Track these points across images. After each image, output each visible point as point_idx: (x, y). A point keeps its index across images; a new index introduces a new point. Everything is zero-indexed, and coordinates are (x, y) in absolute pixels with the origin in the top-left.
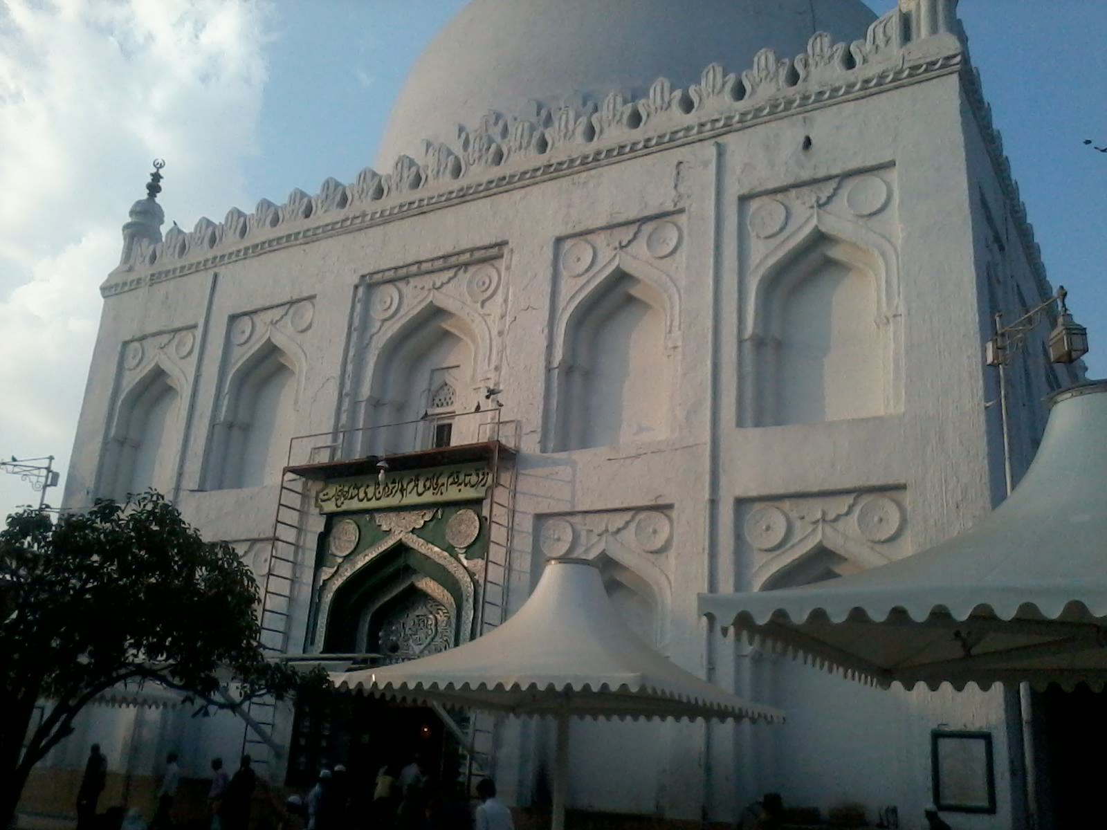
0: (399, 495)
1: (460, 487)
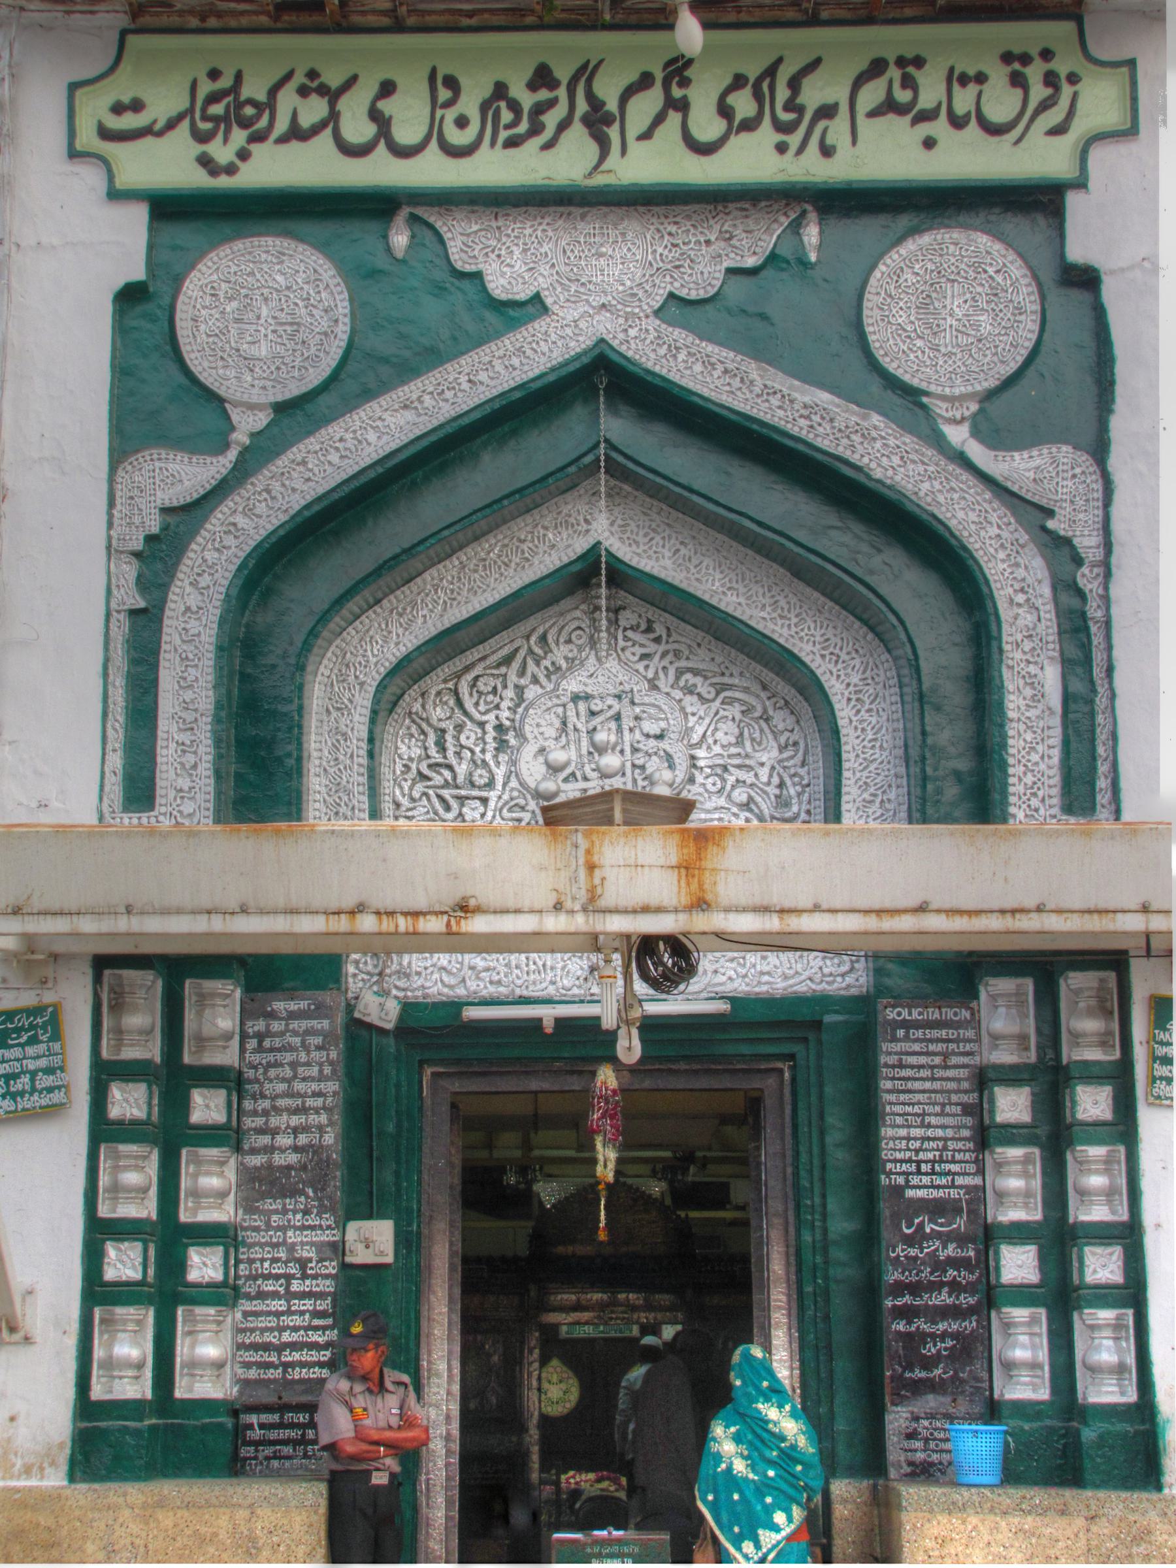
1: (925, 129)
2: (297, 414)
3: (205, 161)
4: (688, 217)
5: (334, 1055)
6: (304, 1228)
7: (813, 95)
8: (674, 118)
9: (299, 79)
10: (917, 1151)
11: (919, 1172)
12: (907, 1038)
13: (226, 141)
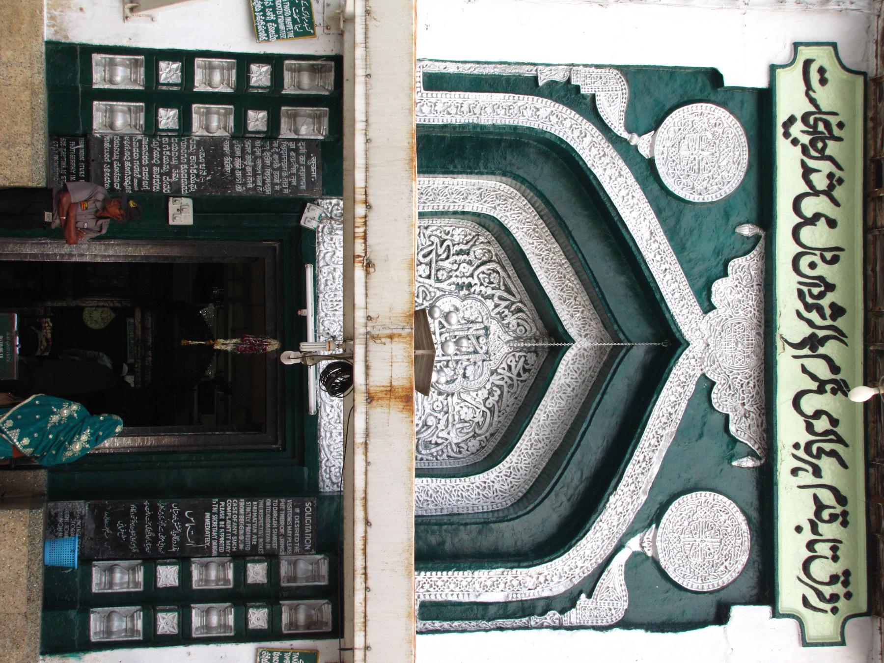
0: (802, 331)
1: (807, 527)
2: (647, 172)
3: (791, 120)
4: (758, 393)
5: (286, 191)
6: (189, 174)
7: (827, 464)
8: (814, 386)
9: (838, 173)
10: (231, 519)
11: (219, 520)
12: (294, 514)
13: (803, 132)
